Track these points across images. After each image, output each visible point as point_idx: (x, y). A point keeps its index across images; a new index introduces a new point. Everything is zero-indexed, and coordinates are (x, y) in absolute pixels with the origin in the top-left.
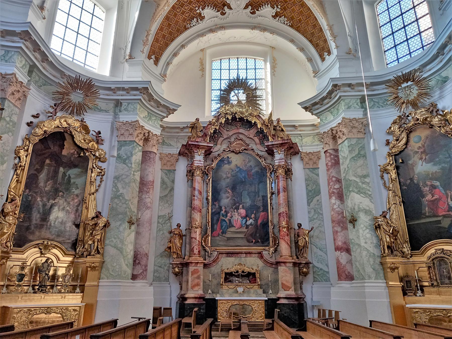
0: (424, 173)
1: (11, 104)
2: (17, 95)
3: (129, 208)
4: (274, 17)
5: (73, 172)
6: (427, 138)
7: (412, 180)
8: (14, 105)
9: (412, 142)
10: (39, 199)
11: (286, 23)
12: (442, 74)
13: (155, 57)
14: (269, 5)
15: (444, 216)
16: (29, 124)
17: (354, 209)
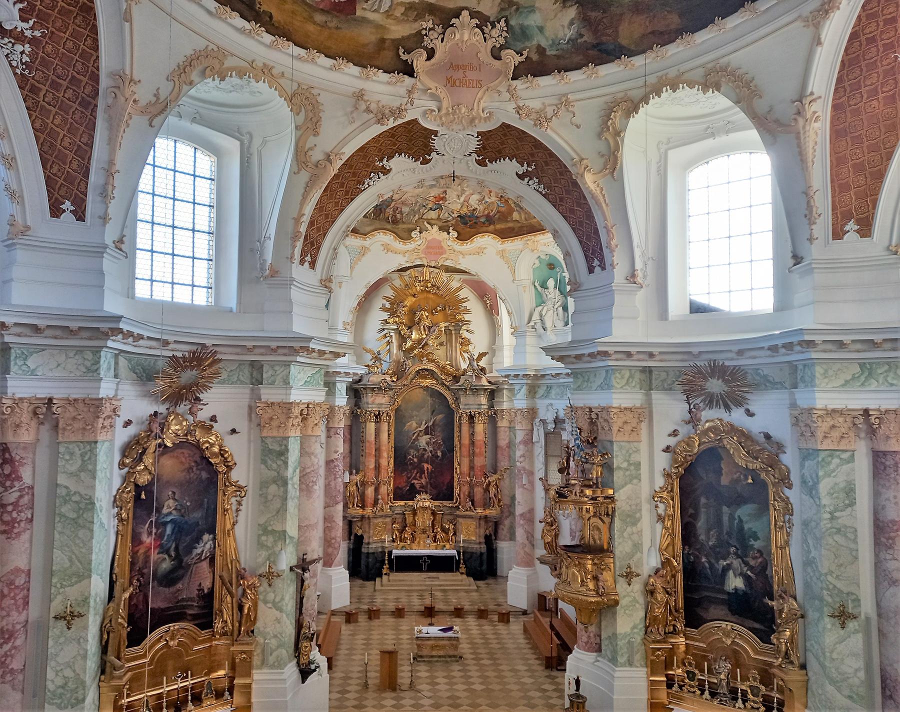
1: (621, 443)
2: (628, 428)
3: (828, 589)
5: (744, 511)
8: (629, 442)
10: (704, 560)
13: (858, 222)
16: (667, 449)
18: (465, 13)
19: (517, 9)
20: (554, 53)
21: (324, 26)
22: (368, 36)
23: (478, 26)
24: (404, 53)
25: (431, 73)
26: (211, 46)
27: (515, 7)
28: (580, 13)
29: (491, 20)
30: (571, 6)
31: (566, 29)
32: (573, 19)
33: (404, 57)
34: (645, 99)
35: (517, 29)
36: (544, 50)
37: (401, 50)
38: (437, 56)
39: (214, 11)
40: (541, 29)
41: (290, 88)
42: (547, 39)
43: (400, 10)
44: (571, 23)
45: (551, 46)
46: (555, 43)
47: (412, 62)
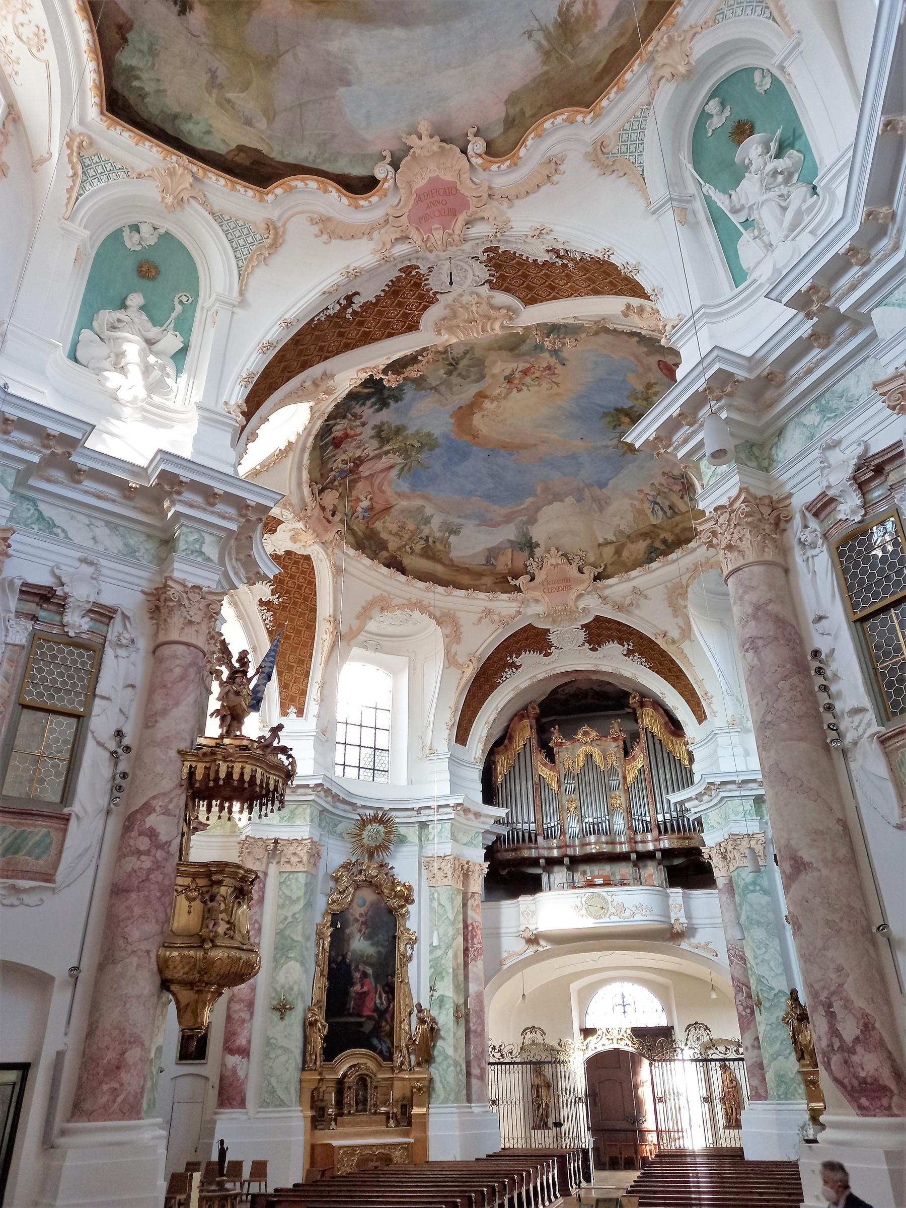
0: (359, 952)
4: (261, 603)
6: (372, 905)
7: (344, 957)
9: (354, 904)
11: (267, 622)
12: (400, 829)
14: (272, 587)
15: (369, 1018)
17: (291, 989)
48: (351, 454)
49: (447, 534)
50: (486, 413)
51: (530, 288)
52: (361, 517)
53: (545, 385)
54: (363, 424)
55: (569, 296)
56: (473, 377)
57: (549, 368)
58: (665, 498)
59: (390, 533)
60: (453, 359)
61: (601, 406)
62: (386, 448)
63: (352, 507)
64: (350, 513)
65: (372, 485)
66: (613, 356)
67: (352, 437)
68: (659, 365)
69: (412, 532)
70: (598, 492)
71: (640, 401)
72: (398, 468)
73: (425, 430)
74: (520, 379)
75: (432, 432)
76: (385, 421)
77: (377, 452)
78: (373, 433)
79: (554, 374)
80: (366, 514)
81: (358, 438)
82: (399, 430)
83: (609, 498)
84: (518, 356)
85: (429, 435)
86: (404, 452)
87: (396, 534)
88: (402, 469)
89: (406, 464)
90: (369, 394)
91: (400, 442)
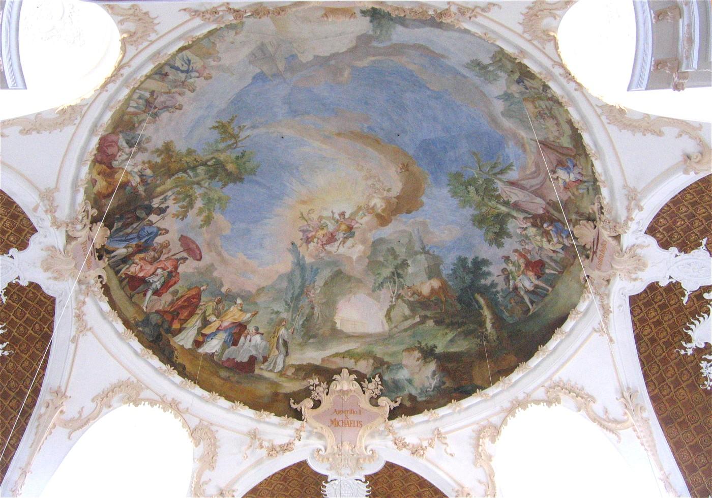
18: (345, 371)
19: (388, 367)
20: (424, 399)
21: (226, 380)
22: (263, 390)
23: (356, 380)
24: (294, 403)
25: (317, 418)
26: (133, 379)
27: (386, 366)
28: (438, 366)
29: (368, 376)
30: (430, 362)
31: (431, 380)
32: (434, 372)
33: (294, 406)
34: (504, 421)
35: (390, 383)
36: (416, 397)
37: (292, 401)
38: (322, 405)
39: (139, 351)
40: (410, 381)
41: (194, 422)
42: (416, 389)
43: (290, 372)
44: (434, 374)
45: (420, 394)
46: (423, 391)
47: (301, 410)
48: (538, 238)
49: (491, 68)
50: (385, 193)
51: (300, 476)
52: (577, 171)
53: (315, 216)
54: (507, 259)
55: (273, 475)
56: (384, 247)
57: (308, 241)
58: (175, 81)
59: (558, 124)
60: (395, 283)
61: (257, 183)
62: (504, 209)
63: (577, 189)
64: (584, 186)
65: (543, 184)
66: (245, 258)
67: (525, 257)
68: (200, 254)
69: (533, 102)
70: (265, 69)
71: (216, 197)
72: (506, 177)
73: (455, 202)
74: (337, 230)
75: (449, 195)
76: (486, 245)
77: (515, 213)
78: (506, 241)
79: (303, 231)
80: (569, 164)
81: (520, 248)
82: (480, 221)
83: (250, 62)
84: (335, 263)
85: (454, 194)
86: (488, 191)
87: (553, 117)
88: (502, 172)
89: (495, 174)
90: (482, 294)
91: (487, 205)
